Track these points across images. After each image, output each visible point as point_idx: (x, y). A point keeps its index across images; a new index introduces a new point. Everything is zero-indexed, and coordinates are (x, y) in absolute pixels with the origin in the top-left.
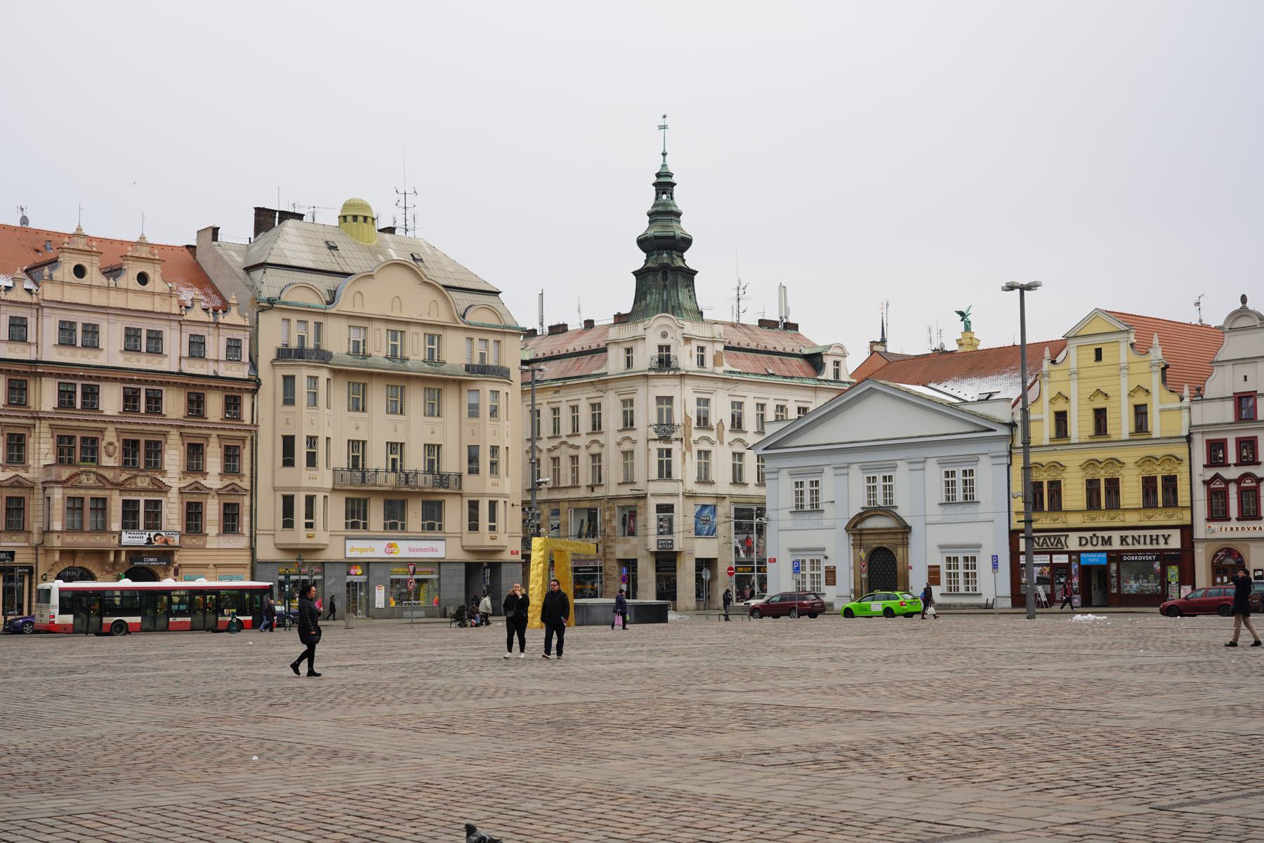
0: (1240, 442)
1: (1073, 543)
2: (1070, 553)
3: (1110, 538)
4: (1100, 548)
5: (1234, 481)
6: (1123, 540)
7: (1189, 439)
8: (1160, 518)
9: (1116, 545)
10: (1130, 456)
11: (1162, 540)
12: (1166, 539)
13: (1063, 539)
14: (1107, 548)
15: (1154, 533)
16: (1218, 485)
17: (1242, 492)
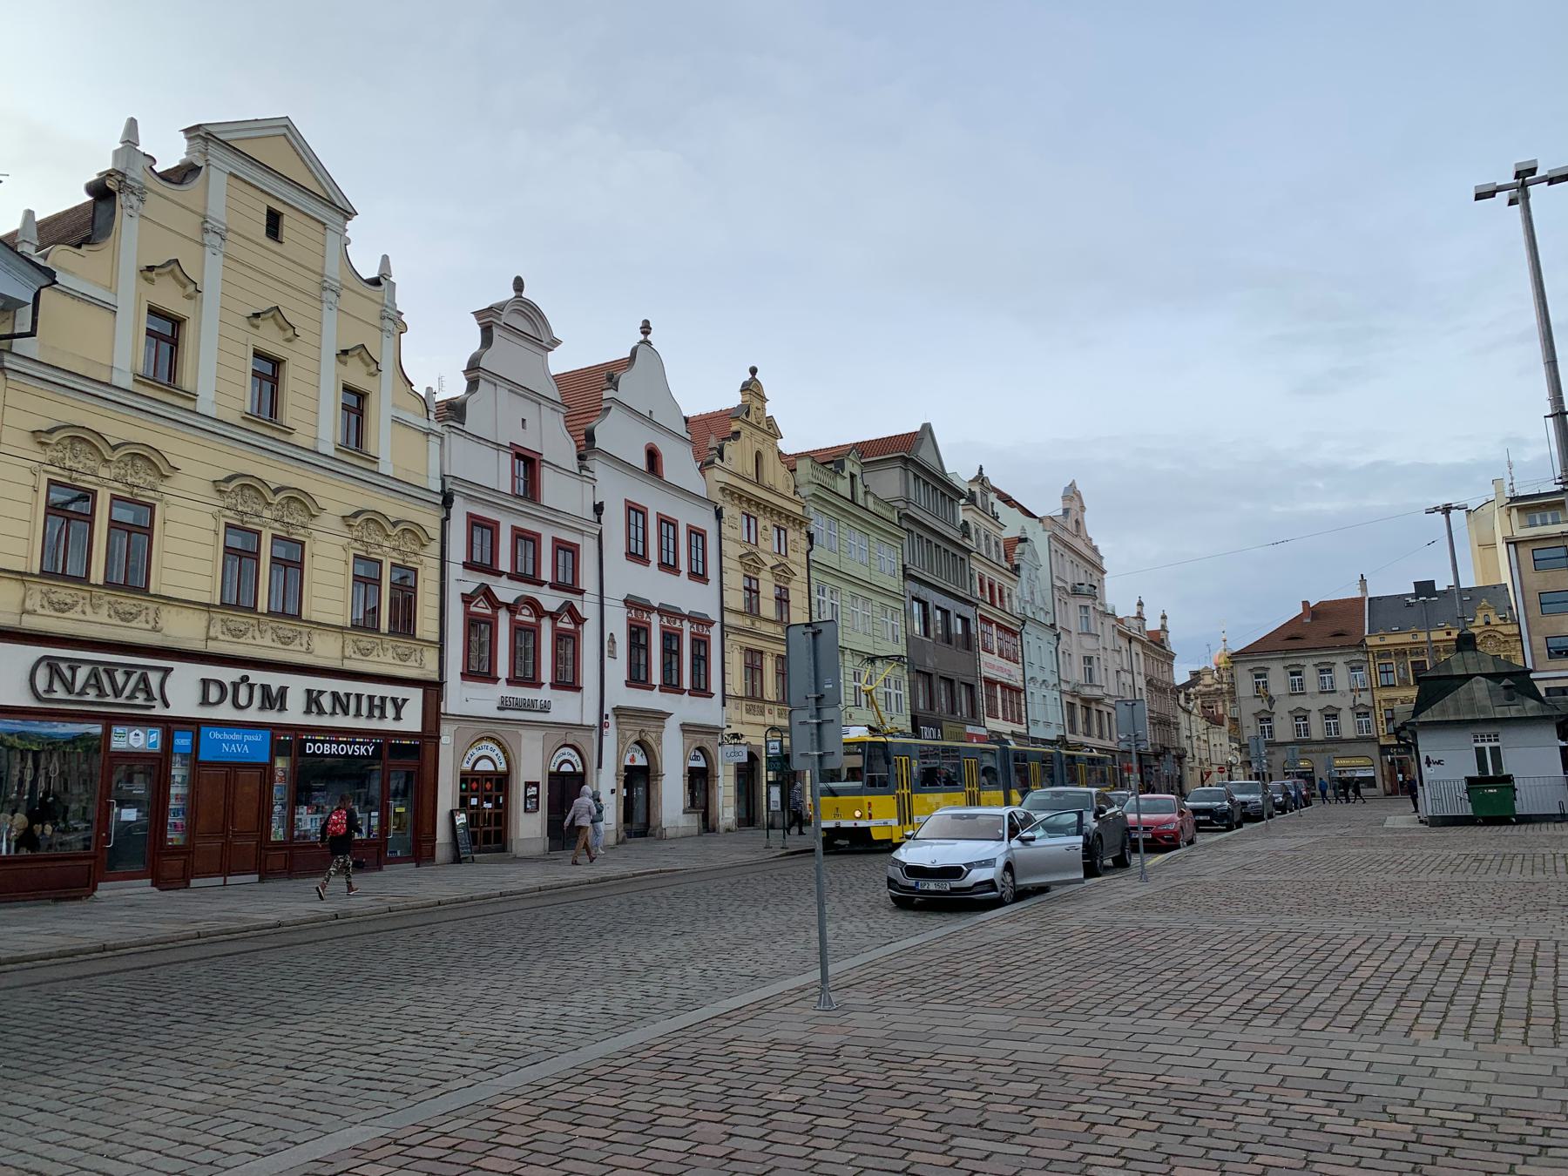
0: (519, 535)
1: (182, 693)
2: (169, 726)
3: (283, 691)
4: (253, 715)
5: (508, 606)
6: (313, 700)
7: (447, 500)
8: (384, 660)
9: (295, 714)
10: (336, 497)
11: (390, 711)
12: (399, 706)
13: (154, 679)
14: (271, 717)
15: (379, 690)
16: (481, 608)
17: (517, 629)
